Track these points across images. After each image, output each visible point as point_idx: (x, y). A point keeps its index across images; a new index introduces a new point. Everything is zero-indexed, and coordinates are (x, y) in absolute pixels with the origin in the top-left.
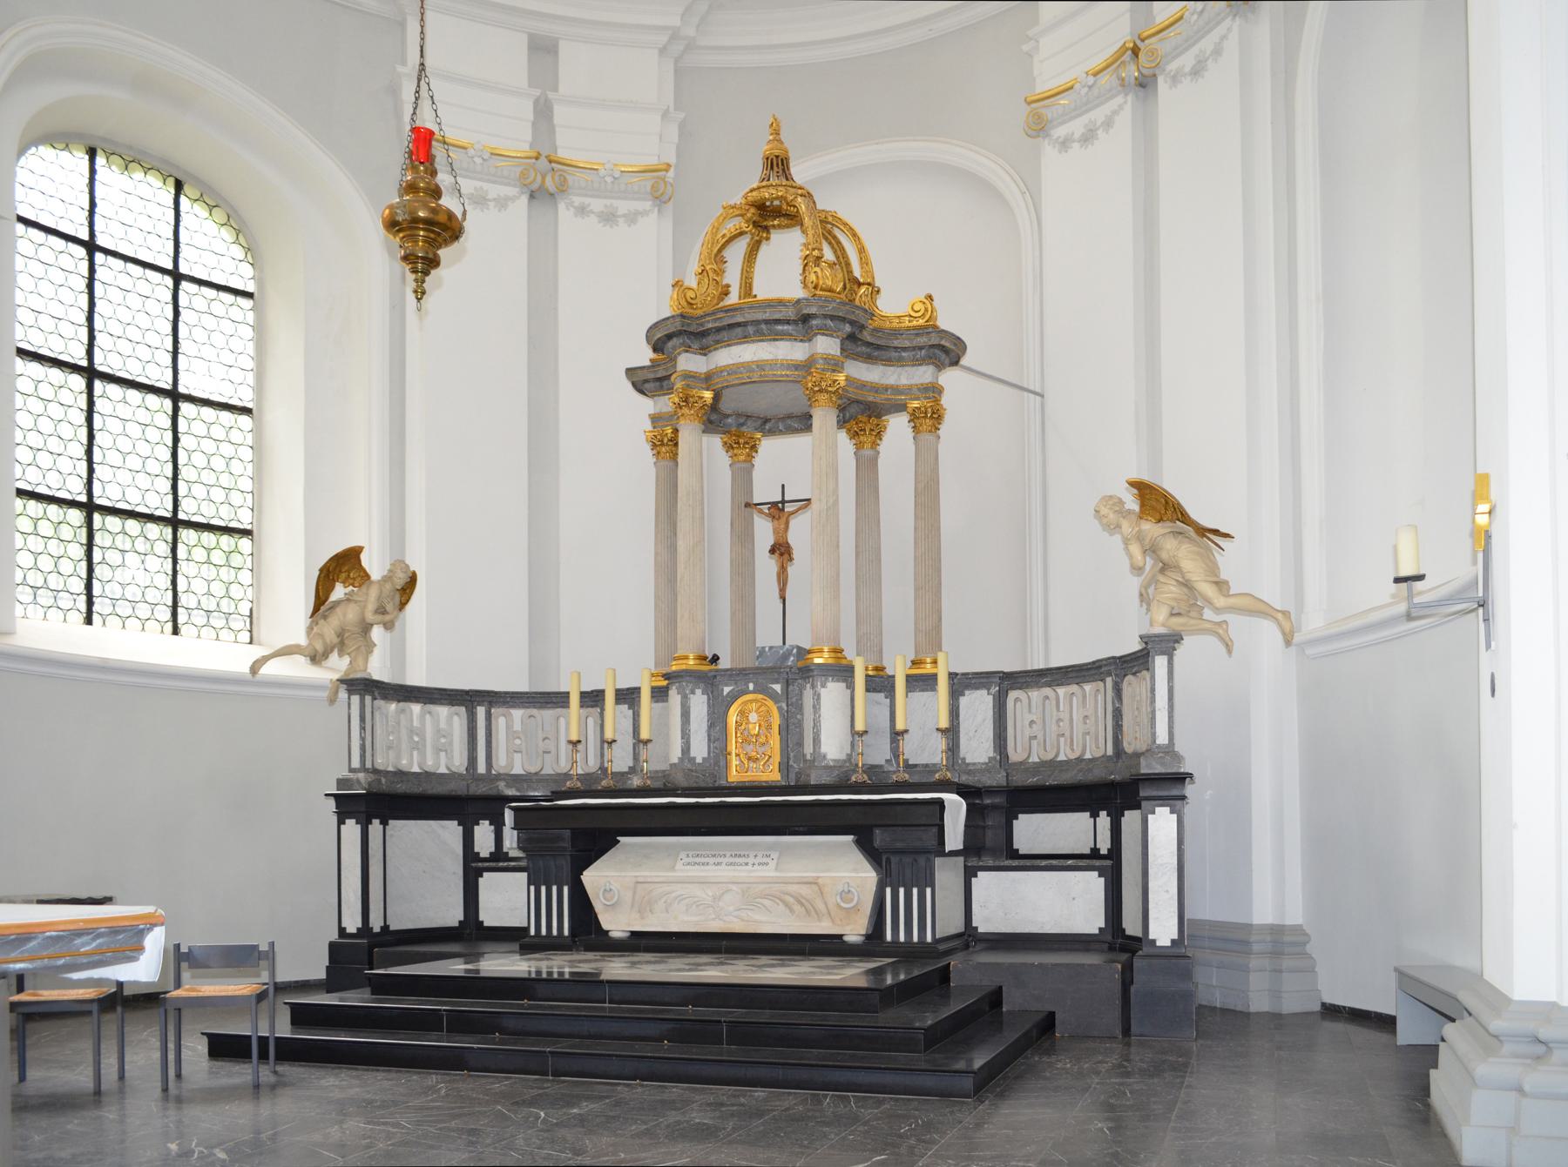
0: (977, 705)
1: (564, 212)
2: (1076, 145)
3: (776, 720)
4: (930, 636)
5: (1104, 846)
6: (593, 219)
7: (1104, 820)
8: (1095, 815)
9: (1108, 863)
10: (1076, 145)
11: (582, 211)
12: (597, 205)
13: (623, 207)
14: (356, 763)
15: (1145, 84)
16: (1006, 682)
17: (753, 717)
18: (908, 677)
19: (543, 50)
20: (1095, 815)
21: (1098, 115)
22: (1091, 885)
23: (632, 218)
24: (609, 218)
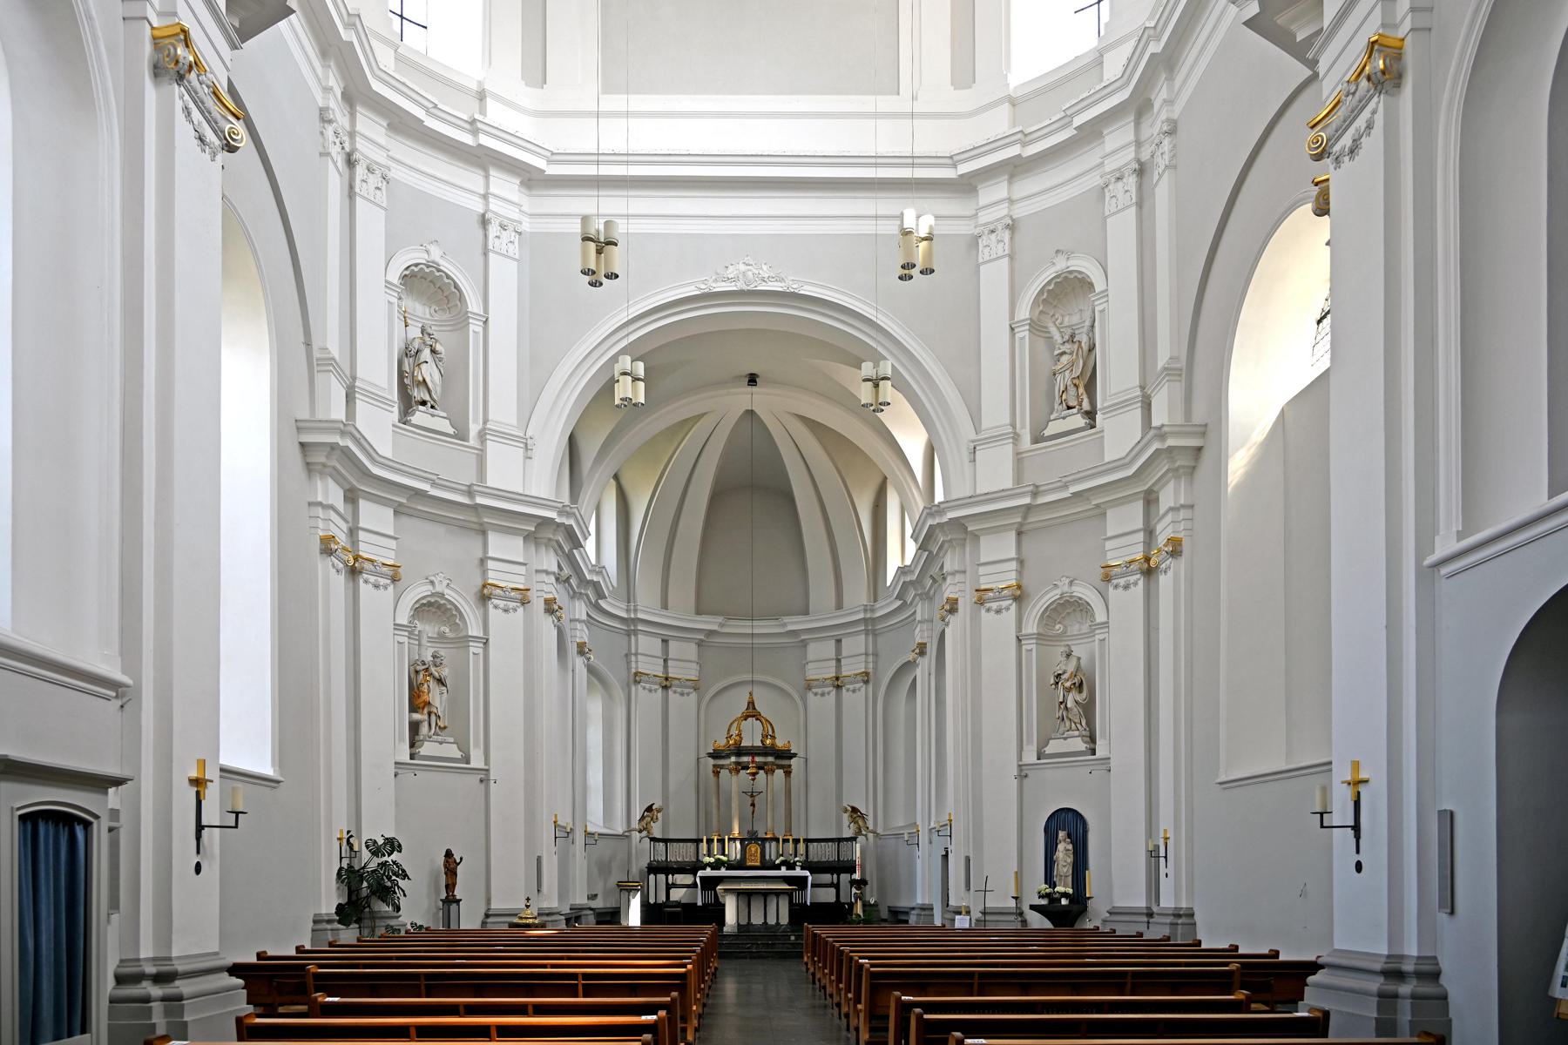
0: (801, 846)
1: (670, 692)
2: (819, 696)
3: (759, 851)
4: (789, 830)
5: (835, 881)
6: (678, 695)
7: (835, 876)
8: (832, 875)
9: (837, 886)
10: (819, 696)
11: (675, 692)
12: (679, 690)
13: (686, 691)
14: (652, 859)
15: (838, 687)
16: (807, 841)
17: (753, 849)
18: (783, 839)
19: (665, 641)
20: (832, 875)
21: (826, 690)
22: (833, 891)
23: (688, 694)
24: (682, 694)
